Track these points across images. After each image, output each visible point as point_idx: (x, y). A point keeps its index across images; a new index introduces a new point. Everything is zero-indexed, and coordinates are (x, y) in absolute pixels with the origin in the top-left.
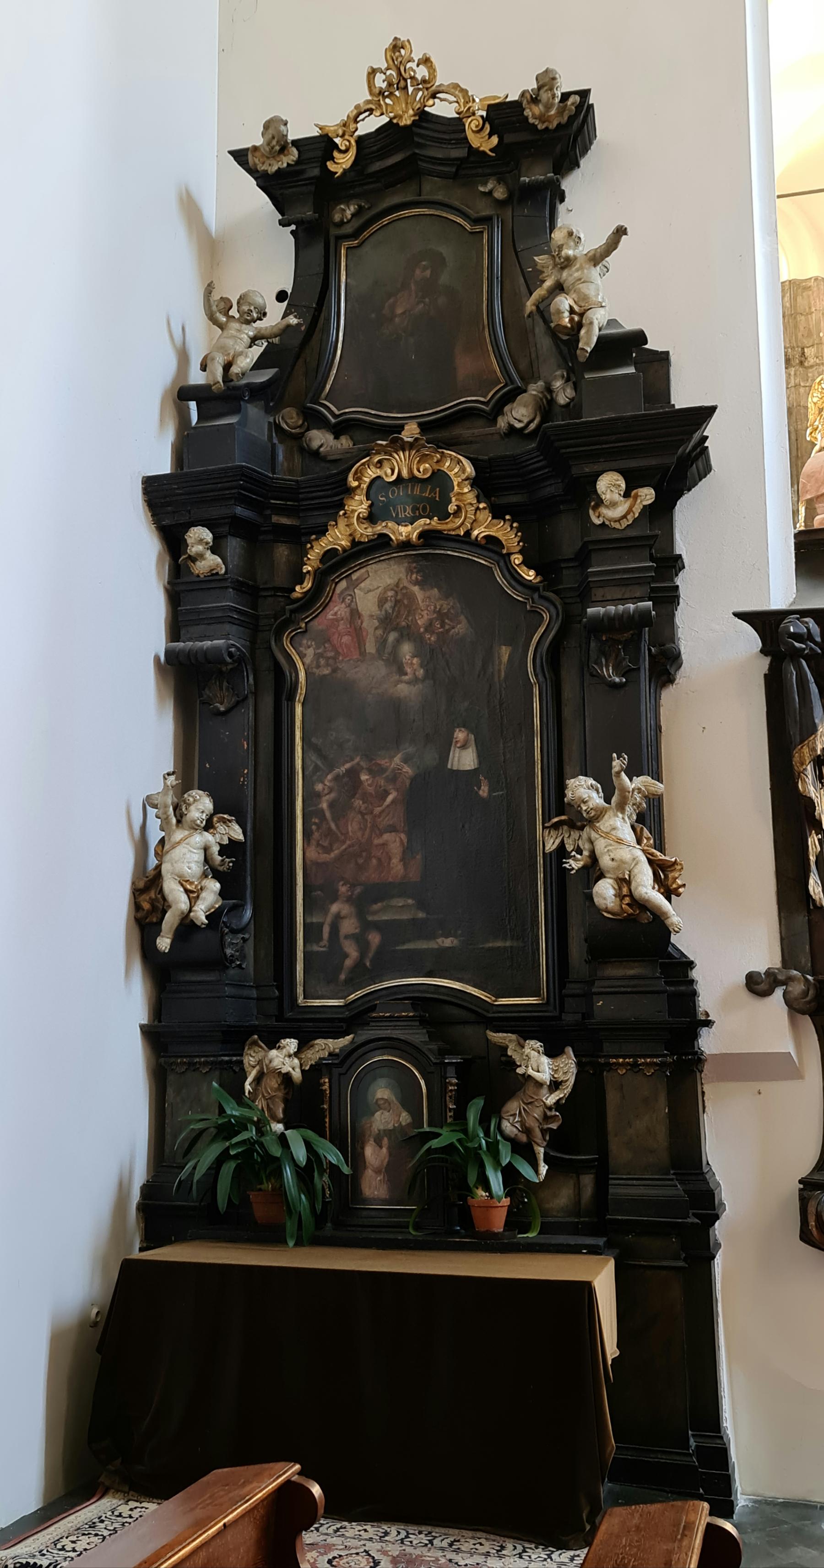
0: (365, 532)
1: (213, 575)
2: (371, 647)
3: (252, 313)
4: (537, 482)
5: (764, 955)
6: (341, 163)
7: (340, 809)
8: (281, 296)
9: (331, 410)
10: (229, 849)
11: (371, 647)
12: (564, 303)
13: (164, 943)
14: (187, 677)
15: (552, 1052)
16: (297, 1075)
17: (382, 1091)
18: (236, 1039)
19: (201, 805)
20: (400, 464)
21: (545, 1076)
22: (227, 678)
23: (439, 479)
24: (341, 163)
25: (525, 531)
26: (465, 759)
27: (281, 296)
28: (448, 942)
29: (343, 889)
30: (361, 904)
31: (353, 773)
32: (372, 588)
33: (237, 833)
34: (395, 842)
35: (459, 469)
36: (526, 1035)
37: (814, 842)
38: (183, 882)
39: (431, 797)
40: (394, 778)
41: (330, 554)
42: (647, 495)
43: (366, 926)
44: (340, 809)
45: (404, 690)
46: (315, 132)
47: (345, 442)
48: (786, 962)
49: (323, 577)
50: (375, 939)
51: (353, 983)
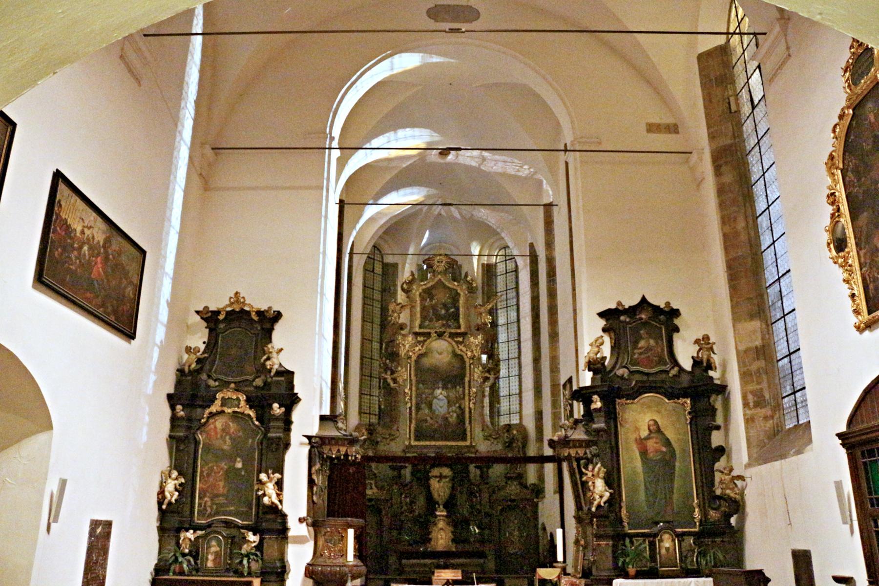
0: (219, 409)
3: (197, 350)
5: (304, 514)
6: (221, 317)
7: (209, 475)
8: (204, 343)
9: (214, 376)
12: (268, 363)
15: (255, 534)
16: (193, 539)
17: (214, 543)
18: (178, 530)
19: (175, 474)
20: (229, 394)
21: (252, 540)
22: (183, 443)
23: (238, 399)
24: (221, 317)
25: (257, 414)
26: (239, 465)
27: (204, 343)
29: (208, 495)
33: (183, 481)
34: (221, 484)
35: (243, 397)
36: (250, 530)
37: (315, 489)
38: (170, 492)
39: (231, 472)
40: (222, 469)
41: (210, 413)
42: (283, 409)
43: (213, 504)
44: (209, 475)
45: (225, 447)
47: (217, 383)
49: (208, 418)
50: (215, 507)
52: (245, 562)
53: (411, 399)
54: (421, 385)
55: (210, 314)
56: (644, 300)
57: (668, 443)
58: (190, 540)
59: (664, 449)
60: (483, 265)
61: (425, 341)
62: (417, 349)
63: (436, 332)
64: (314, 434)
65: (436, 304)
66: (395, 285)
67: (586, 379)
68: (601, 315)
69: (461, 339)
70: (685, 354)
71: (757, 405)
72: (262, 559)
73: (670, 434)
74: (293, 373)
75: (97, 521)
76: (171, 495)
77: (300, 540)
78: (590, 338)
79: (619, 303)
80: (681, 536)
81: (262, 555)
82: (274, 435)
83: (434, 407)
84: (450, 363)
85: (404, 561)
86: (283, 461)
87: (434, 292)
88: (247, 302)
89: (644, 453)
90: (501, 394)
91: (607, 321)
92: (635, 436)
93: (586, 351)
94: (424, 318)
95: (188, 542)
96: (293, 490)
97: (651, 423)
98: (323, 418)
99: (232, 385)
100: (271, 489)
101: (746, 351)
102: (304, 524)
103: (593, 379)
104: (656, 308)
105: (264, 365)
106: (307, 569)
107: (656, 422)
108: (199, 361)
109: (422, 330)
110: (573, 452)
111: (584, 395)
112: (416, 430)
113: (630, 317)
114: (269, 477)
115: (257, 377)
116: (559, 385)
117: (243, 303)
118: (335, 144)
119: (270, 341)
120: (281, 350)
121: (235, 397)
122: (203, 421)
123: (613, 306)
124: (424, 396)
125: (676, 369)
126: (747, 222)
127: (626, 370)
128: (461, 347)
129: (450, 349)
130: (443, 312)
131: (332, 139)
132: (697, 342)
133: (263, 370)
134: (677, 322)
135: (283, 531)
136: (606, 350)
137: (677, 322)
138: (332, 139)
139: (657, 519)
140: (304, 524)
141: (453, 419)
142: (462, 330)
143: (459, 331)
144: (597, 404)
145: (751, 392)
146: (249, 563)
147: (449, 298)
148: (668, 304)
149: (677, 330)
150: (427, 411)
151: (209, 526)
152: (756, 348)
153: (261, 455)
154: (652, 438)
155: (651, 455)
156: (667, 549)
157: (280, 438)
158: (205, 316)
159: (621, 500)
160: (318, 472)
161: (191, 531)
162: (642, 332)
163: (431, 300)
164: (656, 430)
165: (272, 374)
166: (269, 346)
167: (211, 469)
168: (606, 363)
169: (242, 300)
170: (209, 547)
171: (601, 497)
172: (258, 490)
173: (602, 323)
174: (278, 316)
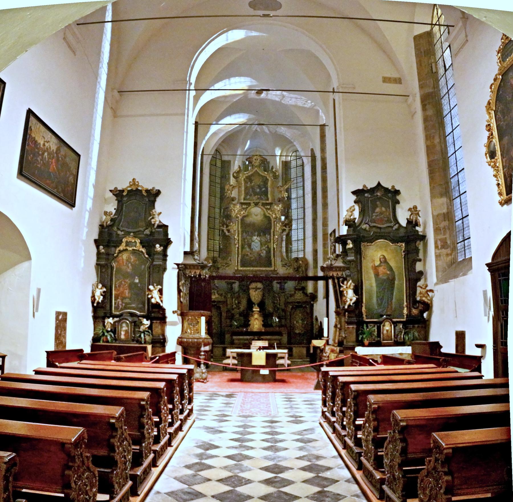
0: (125, 248)
1: (103, 253)
2: (125, 264)
3: (111, 213)
4: (148, 244)
5: (176, 309)
6: (125, 194)
7: (119, 286)
8: (115, 209)
10: (104, 292)
11: (125, 264)
12: (153, 220)
13: (95, 305)
14: (98, 266)
15: (147, 320)
16: (112, 323)
17: (124, 325)
18: (104, 318)
19: (100, 286)
20: (130, 239)
22: (104, 268)
23: (135, 242)
24: (125, 194)
26: (137, 281)
28: (134, 305)
29: (119, 298)
30: (122, 300)
31: (121, 281)
32: (125, 256)
33: (105, 289)
34: (127, 292)
35: (138, 241)
37: (182, 294)
40: (127, 283)
42: (162, 248)
43: (123, 303)
44: (119, 286)
45: (129, 270)
46: (121, 189)
47: (123, 233)
48: (178, 309)
49: (118, 253)
50: (124, 305)
51: (120, 311)
52: (142, 335)
53: (238, 243)
54: (244, 234)
55: (118, 192)
56: (379, 184)
57: (391, 269)
58: (111, 323)
59: (388, 272)
60: (283, 161)
61: (247, 208)
62: (242, 213)
63: (254, 203)
64: (180, 262)
65: (254, 185)
66: (229, 174)
67: (344, 230)
68: (354, 193)
69: (269, 207)
70: (403, 217)
71: (443, 247)
72: (152, 335)
73: (392, 264)
74: (167, 226)
75: (59, 312)
76: (99, 298)
77: (174, 324)
78: (347, 207)
79: (365, 186)
80: (395, 324)
81: (152, 331)
82: (157, 263)
83: (252, 247)
84: (262, 221)
85: (234, 337)
86: (163, 278)
87: (252, 178)
88: (140, 185)
89: (377, 275)
90: (293, 239)
91: (357, 196)
92: (372, 264)
93: (344, 214)
94: (246, 194)
95: (110, 325)
96: (169, 295)
97: (382, 257)
98: (185, 253)
99: (132, 234)
100: (155, 294)
101: (438, 216)
102: (176, 314)
103: (348, 230)
104: (386, 189)
105: (150, 221)
106: (178, 340)
107: (384, 257)
108: (112, 220)
109: (245, 201)
110: (335, 274)
111: (342, 240)
112: (241, 260)
113: (371, 194)
114: (154, 287)
115: (146, 229)
116: (327, 234)
117: (138, 185)
118: (192, 87)
119: (154, 208)
120: (160, 213)
121: (133, 241)
122: (115, 255)
123: (361, 188)
124: (246, 240)
125: (397, 225)
126: (440, 139)
127: (368, 226)
128: (269, 212)
129: (262, 213)
130: (258, 190)
131: (191, 84)
132: (410, 210)
133: (150, 225)
134: (398, 197)
135: (163, 319)
136: (356, 214)
137: (398, 197)
138: (191, 84)
139: (382, 313)
140: (176, 314)
141: (264, 254)
142: (270, 201)
143: (268, 202)
144: (350, 245)
145: (440, 240)
146: (144, 336)
147: (262, 181)
148: (393, 187)
149: (398, 202)
150: (248, 249)
151: (121, 315)
152: (444, 213)
153: (149, 273)
154: (381, 266)
155: (381, 276)
156: (387, 331)
157: (160, 265)
158: (115, 193)
159: (362, 302)
160: (183, 285)
161: (111, 318)
162: (378, 203)
163: (251, 183)
164: (384, 261)
165: (155, 227)
166: (153, 211)
167: (121, 283)
168: (356, 221)
169: (137, 183)
170: (122, 327)
171: (351, 300)
172: (148, 295)
173: (354, 198)
174: (158, 193)
